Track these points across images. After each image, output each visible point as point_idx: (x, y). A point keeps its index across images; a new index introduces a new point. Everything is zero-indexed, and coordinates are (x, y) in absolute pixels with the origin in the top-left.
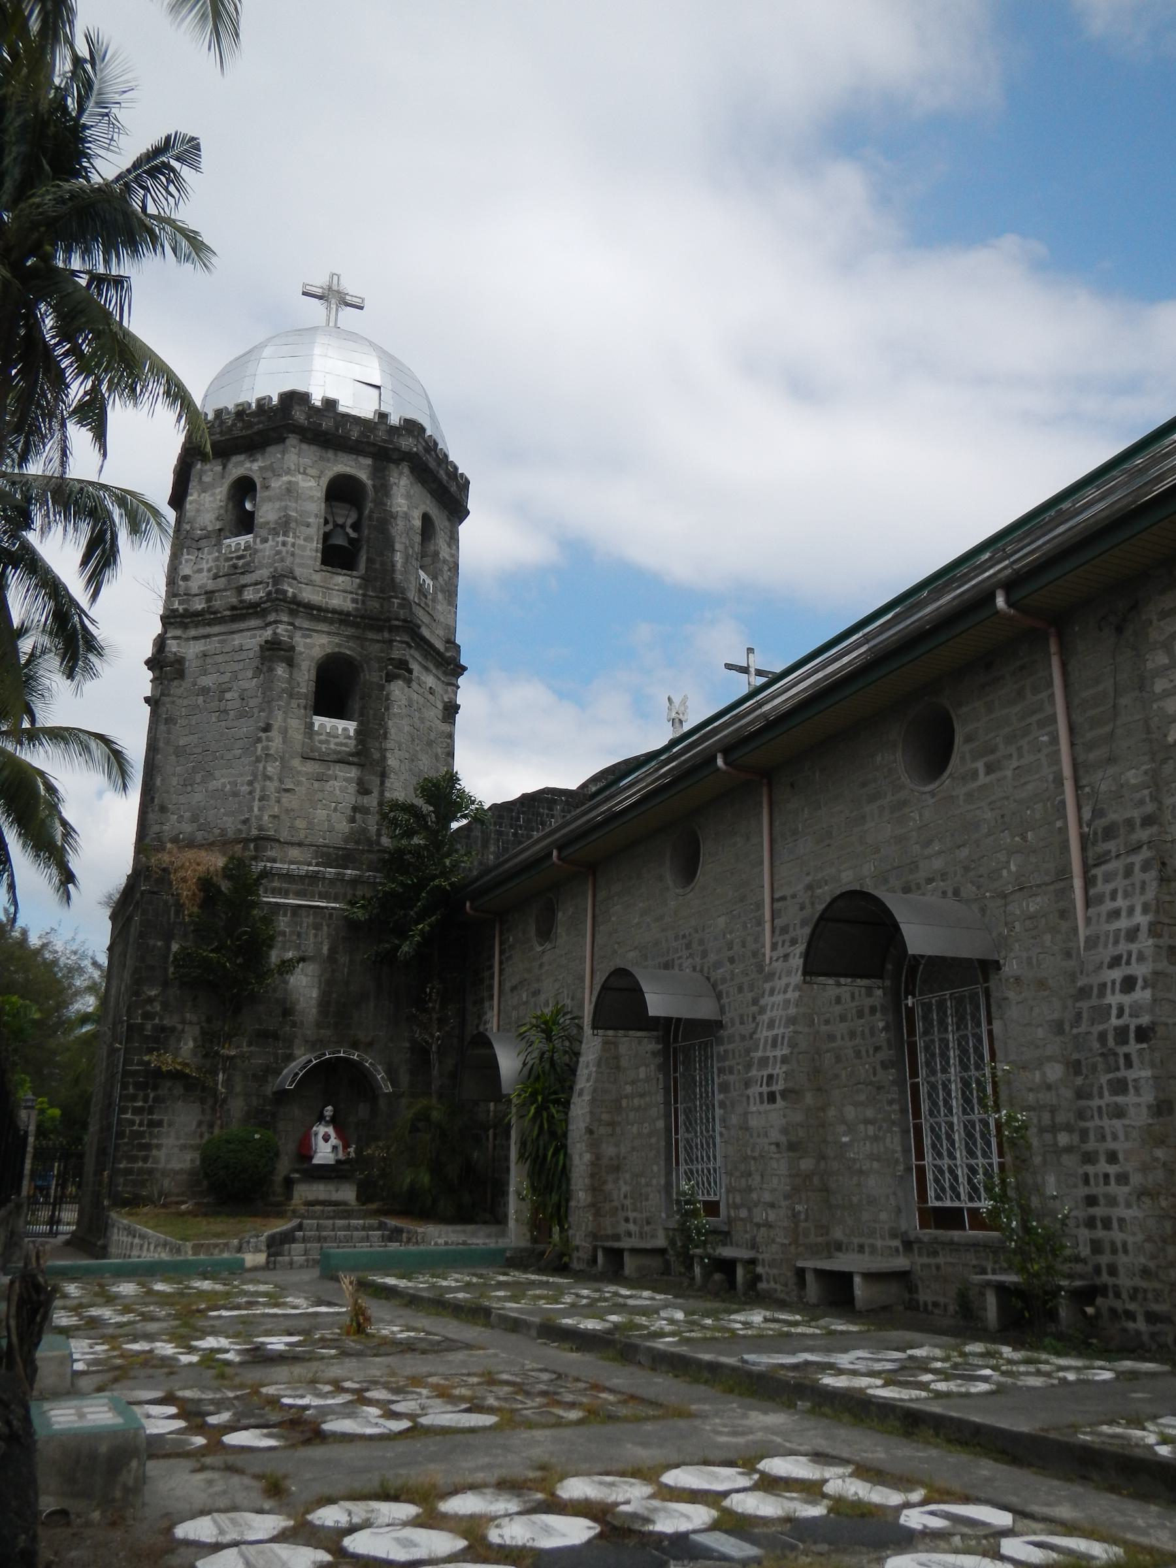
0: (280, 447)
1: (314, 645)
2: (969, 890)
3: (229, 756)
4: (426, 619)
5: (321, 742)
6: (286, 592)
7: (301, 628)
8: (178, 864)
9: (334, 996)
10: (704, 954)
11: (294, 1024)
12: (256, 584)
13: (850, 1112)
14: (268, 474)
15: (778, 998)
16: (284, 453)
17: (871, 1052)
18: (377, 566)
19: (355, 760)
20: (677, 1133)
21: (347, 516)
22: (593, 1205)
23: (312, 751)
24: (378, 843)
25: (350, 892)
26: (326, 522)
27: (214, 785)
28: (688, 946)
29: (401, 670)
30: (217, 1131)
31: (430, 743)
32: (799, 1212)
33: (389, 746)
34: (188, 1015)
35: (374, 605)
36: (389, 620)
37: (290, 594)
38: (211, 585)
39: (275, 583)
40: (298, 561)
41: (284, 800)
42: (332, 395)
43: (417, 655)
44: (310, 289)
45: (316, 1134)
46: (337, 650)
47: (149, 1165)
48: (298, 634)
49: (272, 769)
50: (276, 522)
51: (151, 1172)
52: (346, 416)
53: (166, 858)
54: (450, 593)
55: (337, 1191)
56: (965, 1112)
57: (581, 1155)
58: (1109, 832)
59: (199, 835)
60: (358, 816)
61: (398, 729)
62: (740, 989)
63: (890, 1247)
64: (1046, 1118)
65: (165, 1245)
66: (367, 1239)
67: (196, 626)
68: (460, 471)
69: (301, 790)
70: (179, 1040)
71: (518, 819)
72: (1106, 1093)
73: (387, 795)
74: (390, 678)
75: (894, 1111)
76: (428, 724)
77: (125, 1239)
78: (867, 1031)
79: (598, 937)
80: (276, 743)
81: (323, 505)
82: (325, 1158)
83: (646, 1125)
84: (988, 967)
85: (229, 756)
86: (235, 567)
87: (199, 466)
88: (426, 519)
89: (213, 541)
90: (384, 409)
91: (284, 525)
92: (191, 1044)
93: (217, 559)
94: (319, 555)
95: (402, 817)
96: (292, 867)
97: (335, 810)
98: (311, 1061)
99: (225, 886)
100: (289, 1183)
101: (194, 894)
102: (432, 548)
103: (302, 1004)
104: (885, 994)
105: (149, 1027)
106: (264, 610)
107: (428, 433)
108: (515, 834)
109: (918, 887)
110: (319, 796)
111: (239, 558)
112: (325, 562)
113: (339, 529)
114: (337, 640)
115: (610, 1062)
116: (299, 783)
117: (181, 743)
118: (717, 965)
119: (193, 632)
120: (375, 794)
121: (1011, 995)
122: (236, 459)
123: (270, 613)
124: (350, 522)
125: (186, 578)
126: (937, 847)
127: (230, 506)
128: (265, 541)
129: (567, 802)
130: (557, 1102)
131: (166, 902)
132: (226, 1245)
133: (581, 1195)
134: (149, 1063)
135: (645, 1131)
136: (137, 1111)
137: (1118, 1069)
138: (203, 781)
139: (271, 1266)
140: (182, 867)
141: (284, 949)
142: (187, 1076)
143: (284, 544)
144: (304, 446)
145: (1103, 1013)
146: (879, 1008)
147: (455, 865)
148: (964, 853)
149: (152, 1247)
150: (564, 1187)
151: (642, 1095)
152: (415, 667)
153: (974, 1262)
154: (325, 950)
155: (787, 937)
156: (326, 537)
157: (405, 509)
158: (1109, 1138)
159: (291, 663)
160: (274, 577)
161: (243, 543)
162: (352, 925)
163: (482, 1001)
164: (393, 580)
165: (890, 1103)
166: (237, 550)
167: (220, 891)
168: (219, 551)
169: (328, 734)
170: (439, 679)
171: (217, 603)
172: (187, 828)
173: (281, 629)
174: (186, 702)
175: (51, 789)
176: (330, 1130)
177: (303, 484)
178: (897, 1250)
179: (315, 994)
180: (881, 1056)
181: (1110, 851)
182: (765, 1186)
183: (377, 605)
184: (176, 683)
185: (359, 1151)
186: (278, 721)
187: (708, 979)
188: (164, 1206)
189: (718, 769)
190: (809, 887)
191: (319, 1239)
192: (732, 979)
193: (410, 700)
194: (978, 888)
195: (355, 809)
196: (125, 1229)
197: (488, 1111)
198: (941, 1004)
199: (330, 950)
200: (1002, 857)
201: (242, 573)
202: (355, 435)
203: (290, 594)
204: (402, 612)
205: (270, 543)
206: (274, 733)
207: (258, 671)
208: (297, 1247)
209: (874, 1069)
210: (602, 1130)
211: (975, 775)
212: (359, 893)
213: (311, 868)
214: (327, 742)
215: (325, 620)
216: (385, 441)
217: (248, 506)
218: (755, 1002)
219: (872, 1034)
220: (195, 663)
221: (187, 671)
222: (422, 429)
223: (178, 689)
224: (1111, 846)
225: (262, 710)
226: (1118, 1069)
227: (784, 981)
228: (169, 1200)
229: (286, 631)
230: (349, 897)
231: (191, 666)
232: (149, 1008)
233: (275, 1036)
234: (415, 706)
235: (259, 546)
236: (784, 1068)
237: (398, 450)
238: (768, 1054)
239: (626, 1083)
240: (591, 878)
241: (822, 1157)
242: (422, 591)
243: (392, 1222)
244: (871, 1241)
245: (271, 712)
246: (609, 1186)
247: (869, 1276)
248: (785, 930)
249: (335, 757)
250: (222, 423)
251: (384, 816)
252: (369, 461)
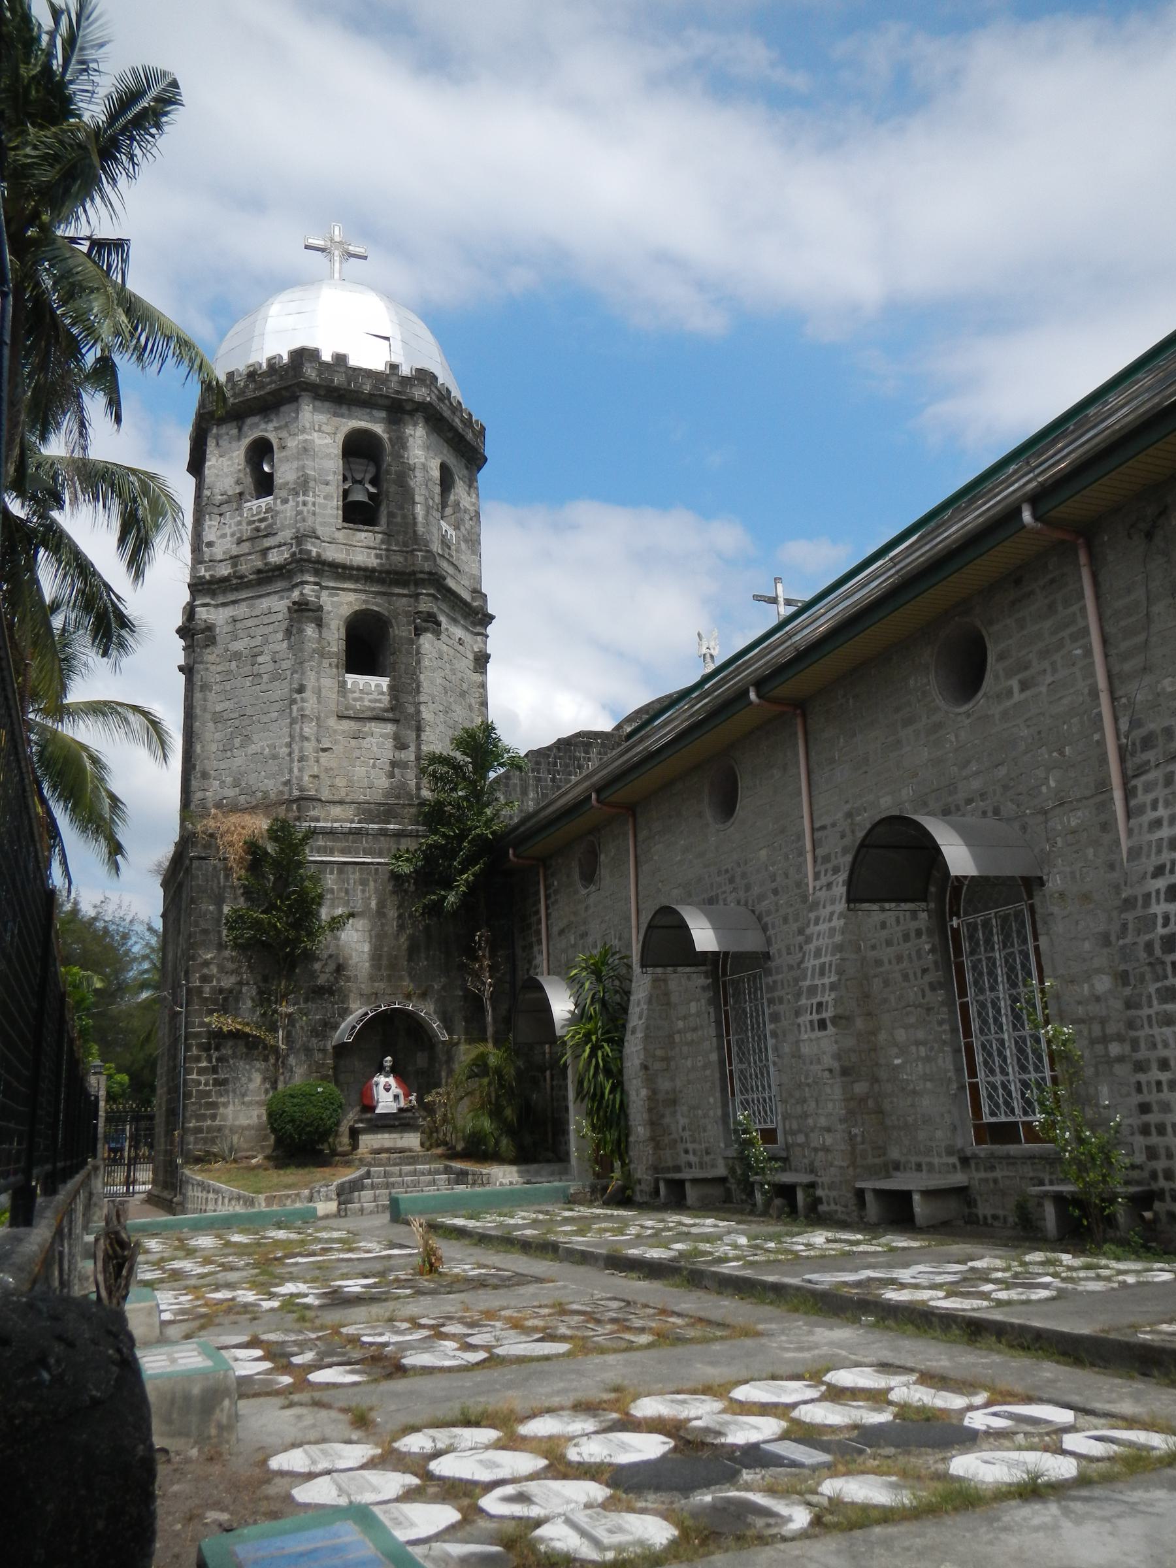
0: (295, 404)
1: (341, 604)
2: (1009, 808)
3: (265, 719)
4: (451, 570)
5: (355, 700)
6: (310, 551)
7: (327, 588)
8: (223, 828)
9: (386, 949)
10: (748, 888)
11: (348, 979)
12: (280, 546)
13: (901, 1035)
14: (284, 434)
15: (823, 927)
16: (297, 412)
17: (919, 975)
18: (399, 519)
19: (390, 715)
20: (730, 1064)
21: (366, 471)
22: (652, 1139)
23: (347, 709)
24: (418, 797)
25: (394, 847)
26: (345, 479)
27: (253, 748)
28: (732, 880)
29: (430, 623)
30: (280, 1086)
31: (463, 694)
32: (856, 1135)
33: (422, 699)
35: (398, 559)
36: (414, 573)
37: (314, 554)
38: (235, 551)
39: (299, 543)
40: (319, 520)
41: (322, 760)
42: (341, 351)
43: (444, 607)
44: (312, 242)
45: (377, 1084)
46: (364, 607)
47: (217, 1123)
48: (325, 593)
49: (309, 729)
50: (296, 483)
51: (219, 1129)
52: (355, 369)
53: (212, 823)
54: (473, 542)
56: (1015, 1028)
57: (637, 1091)
58: (1148, 742)
59: (242, 799)
60: (396, 771)
61: (431, 680)
62: (785, 920)
63: (948, 1164)
64: (1097, 1030)
65: (239, 1198)
66: (434, 1183)
67: (224, 592)
68: (474, 419)
69: (338, 749)
70: (237, 1000)
71: (555, 764)
72: (1155, 1002)
73: (424, 748)
74: (419, 632)
75: (944, 1031)
76: (460, 675)
77: (200, 1194)
78: (914, 954)
79: (641, 877)
80: (310, 703)
81: (341, 462)
82: (387, 1107)
83: (700, 1058)
84: (1032, 884)
85: (265, 719)
86: (257, 530)
87: (214, 431)
88: (444, 468)
89: (235, 505)
90: (395, 359)
91: (303, 485)
92: (249, 1004)
93: (239, 523)
94: (340, 512)
95: (442, 770)
96: (336, 825)
97: (374, 766)
98: (367, 1014)
99: (271, 848)
100: (354, 1134)
101: (241, 858)
102: (452, 498)
103: (355, 959)
104: (930, 917)
105: (207, 989)
106: (289, 571)
107: (440, 381)
108: (553, 780)
109: (958, 808)
110: (357, 753)
111: (261, 520)
112: (346, 519)
113: (359, 486)
114: (363, 597)
115: (661, 999)
116: (336, 742)
117: (218, 709)
118: (761, 897)
119: (221, 600)
120: (412, 748)
121: (1055, 910)
122: (250, 421)
123: (295, 574)
124: (368, 477)
125: (210, 544)
126: (974, 767)
127: (248, 470)
128: (285, 501)
129: (603, 745)
130: (610, 1041)
131: (215, 867)
132: (297, 1195)
133: (640, 1130)
134: (209, 1025)
135: (699, 1064)
136: (201, 1071)
137: (1166, 977)
138: (242, 746)
139: (343, 1213)
140: (227, 831)
141: (333, 906)
142: (247, 1035)
143: (305, 504)
144: (318, 403)
145: (1148, 923)
146: (924, 929)
147: (496, 815)
148: (1002, 771)
149: (226, 1201)
150: (622, 1123)
151: (695, 1029)
152: (442, 619)
153: (1031, 1174)
154: (373, 904)
155: (829, 866)
156: (346, 493)
157: (423, 460)
158: (1160, 1046)
159: (319, 624)
160: (297, 537)
161: (263, 505)
162: (397, 878)
163: (531, 946)
164: (415, 532)
165: (940, 1023)
166: (258, 513)
167: (267, 853)
168: (241, 515)
169: (361, 691)
170: (468, 630)
171: (243, 568)
172: (230, 793)
173: (308, 589)
174: (219, 668)
175: (95, 761)
176: (391, 1080)
177: (318, 442)
178: (954, 1166)
179: (366, 948)
180: (928, 978)
181: (1149, 761)
182: (820, 1111)
183: (401, 559)
184: (208, 650)
185: (420, 1099)
186: (310, 681)
187: (753, 911)
188: (235, 1161)
189: (751, 703)
190: (849, 815)
191: (388, 1186)
192: (777, 911)
193: (440, 651)
194: (1018, 806)
195: (394, 764)
196: (198, 1185)
197: (544, 1053)
198: (986, 924)
199: (377, 904)
200: (1041, 773)
201: (266, 536)
202: (367, 388)
203: (314, 554)
204: (426, 564)
205: (291, 503)
206: (308, 694)
207: (288, 633)
208: (367, 1194)
209: (923, 991)
210: (658, 1066)
211: (1009, 693)
212: (403, 847)
213: (354, 825)
214: (361, 699)
215: (350, 578)
216: (398, 392)
217: (266, 469)
218: (801, 931)
219: (919, 957)
220: (227, 629)
221: (218, 638)
222: (434, 378)
223: (211, 656)
224: (1150, 756)
225: (296, 672)
226: (1166, 977)
227: (829, 909)
228: (240, 1155)
229: (313, 591)
230: (393, 851)
231: (222, 630)
232: (205, 971)
233: (331, 993)
234: (446, 657)
235: (279, 507)
236: (833, 995)
237: (412, 401)
238: (817, 982)
239: (678, 1019)
240: (631, 820)
241: (875, 1080)
242: (445, 543)
243: (458, 1165)
244: (928, 1159)
245: (303, 673)
246: (667, 1120)
247: (927, 1194)
248: (827, 859)
249: (369, 714)
250: (235, 384)
251: (423, 771)
252: (383, 414)
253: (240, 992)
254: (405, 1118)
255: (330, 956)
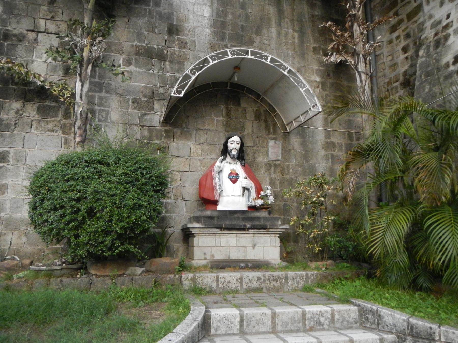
9: (230, 17)
11: (183, 45)
34: (42, 22)
45: (219, 172)
55: (254, 246)
176: (238, 168)
179: (207, 12)
233: (162, 58)
253: (36, 40)
254: (258, 218)
255: (160, 15)
